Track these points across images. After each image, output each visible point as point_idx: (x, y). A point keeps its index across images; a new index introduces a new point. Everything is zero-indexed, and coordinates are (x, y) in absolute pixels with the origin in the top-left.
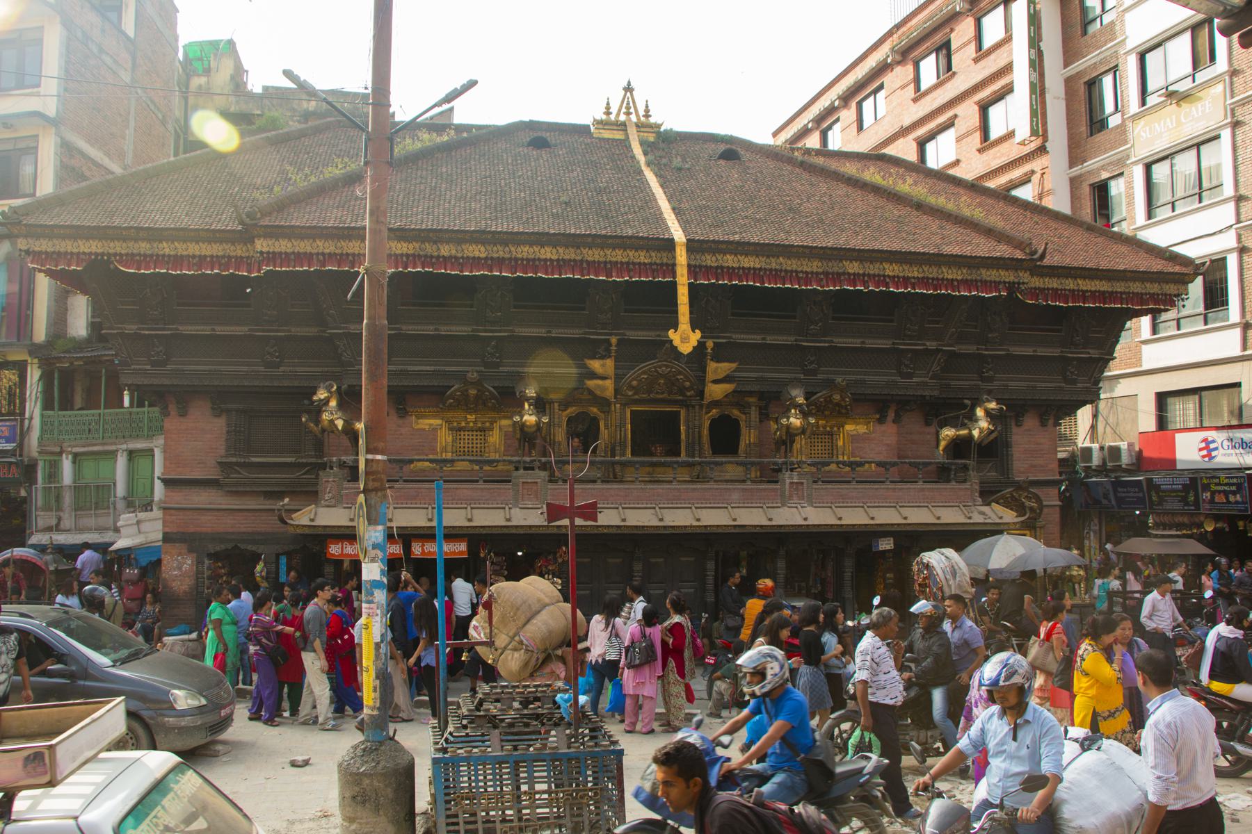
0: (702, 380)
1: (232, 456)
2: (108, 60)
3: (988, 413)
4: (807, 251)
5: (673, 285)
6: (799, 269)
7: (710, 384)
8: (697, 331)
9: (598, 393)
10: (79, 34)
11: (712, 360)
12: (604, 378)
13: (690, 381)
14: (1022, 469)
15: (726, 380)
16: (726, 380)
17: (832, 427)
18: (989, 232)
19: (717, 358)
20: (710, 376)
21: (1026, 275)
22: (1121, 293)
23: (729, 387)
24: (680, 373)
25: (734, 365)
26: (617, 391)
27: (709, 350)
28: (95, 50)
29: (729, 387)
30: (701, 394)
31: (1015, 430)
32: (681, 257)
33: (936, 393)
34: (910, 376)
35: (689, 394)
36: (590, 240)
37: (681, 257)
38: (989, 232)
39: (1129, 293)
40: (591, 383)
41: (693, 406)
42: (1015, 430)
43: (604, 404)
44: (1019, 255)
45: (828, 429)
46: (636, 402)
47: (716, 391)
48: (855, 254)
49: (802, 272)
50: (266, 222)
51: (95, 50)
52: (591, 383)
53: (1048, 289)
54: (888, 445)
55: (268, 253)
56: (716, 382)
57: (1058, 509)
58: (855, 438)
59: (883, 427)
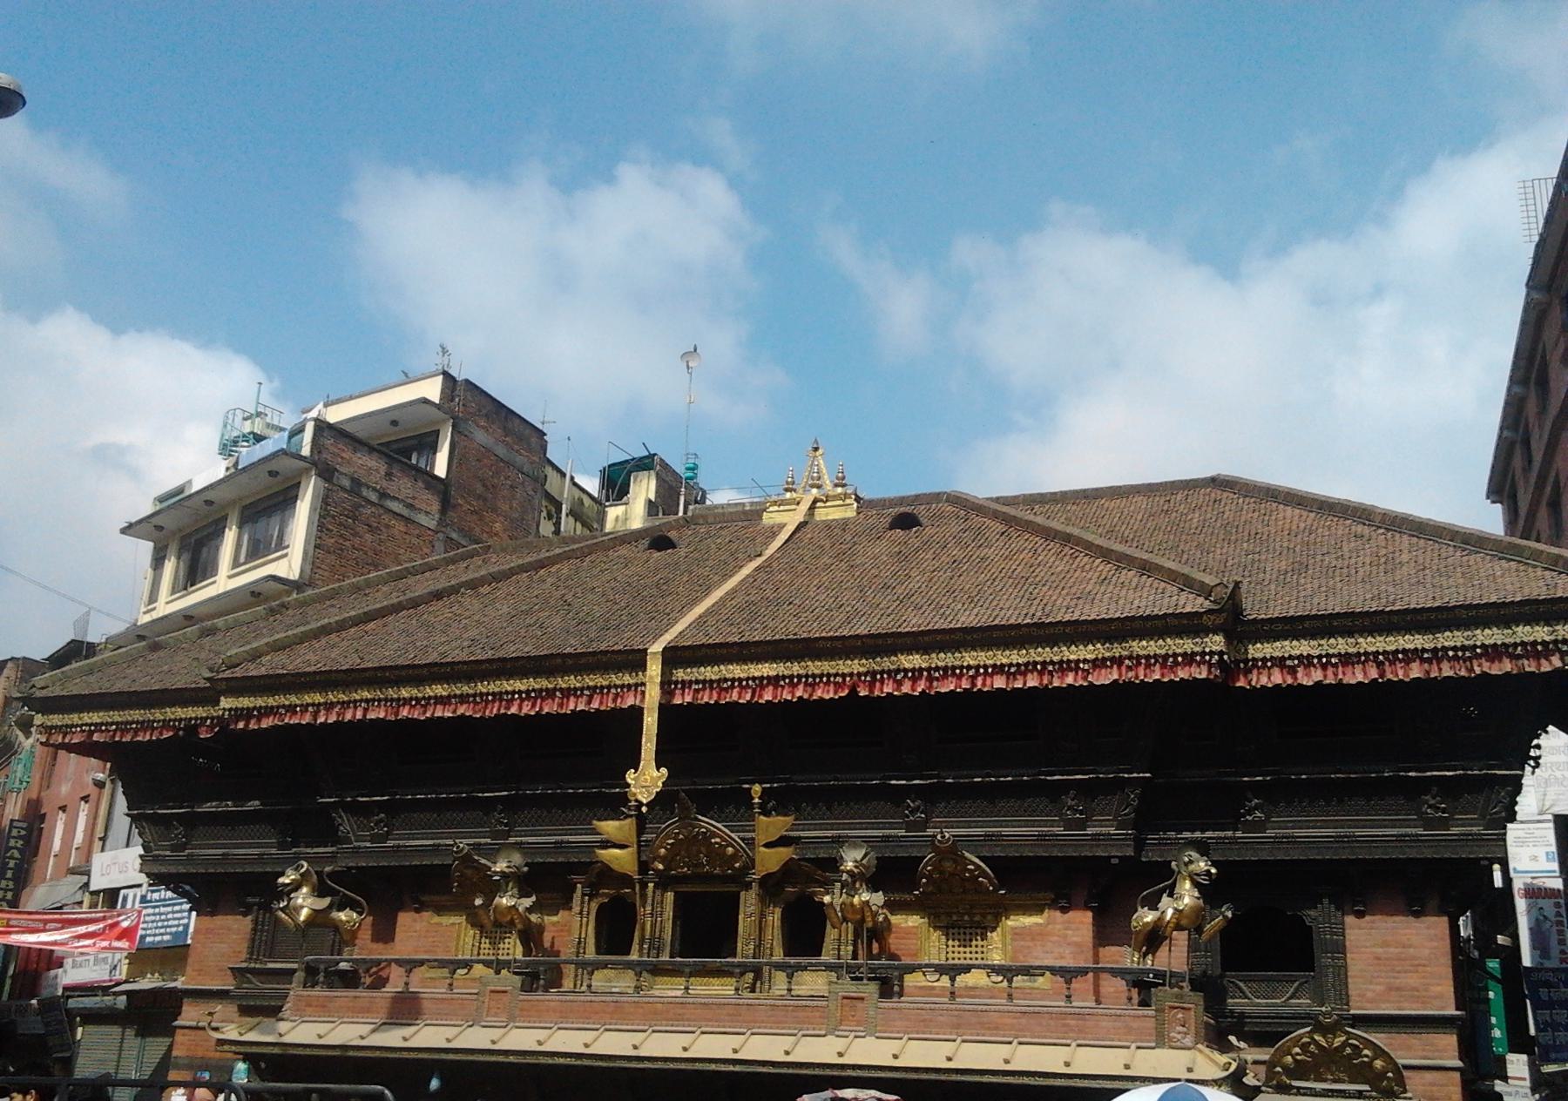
0: (750, 843)
1: (249, 960)
2: (395, 506)
3: (1196, 884)
4: (838, 644)
5: (637, 713)
6: (834, 671)
7: (762, 849)
8: (664, 770)
9: (615, 866)
10: (346, 483)
11: (760, 813)
13: (733, 846)
14: (1369, 994)
15: (783, 841)
16: (783, 841)
17: (984, 916)
18: (1172, 577)
19: (766, 813)
20: (762, 838)
22: (1455, 649)
23: (785, 853)
24: (714, 835)
25: (790, 819)
26: (644, 867)
27: (757, 800)
28: (373, 497)
29: (785, 853)
30: (750, 864)
31: (1350, 920)
32: (654, 669)
33: (1130, 852)
34: (1082, 825)
35: (737, 865)
36: (559, 661)
37: (654, 669)
38: (1172, 577)
39: (1475, 646)
41: (751, 883)
43: (625, 880)
44: (1192, 603)
45: (977, 918)
47: (770, 860)
48: (909, 641)
49: (836, 675)
50: (227, 674)
53: (1291, 657)
54: (1077, 944)
55: (230, 710)
57: (1457, 1075)
58: (1018, 933)
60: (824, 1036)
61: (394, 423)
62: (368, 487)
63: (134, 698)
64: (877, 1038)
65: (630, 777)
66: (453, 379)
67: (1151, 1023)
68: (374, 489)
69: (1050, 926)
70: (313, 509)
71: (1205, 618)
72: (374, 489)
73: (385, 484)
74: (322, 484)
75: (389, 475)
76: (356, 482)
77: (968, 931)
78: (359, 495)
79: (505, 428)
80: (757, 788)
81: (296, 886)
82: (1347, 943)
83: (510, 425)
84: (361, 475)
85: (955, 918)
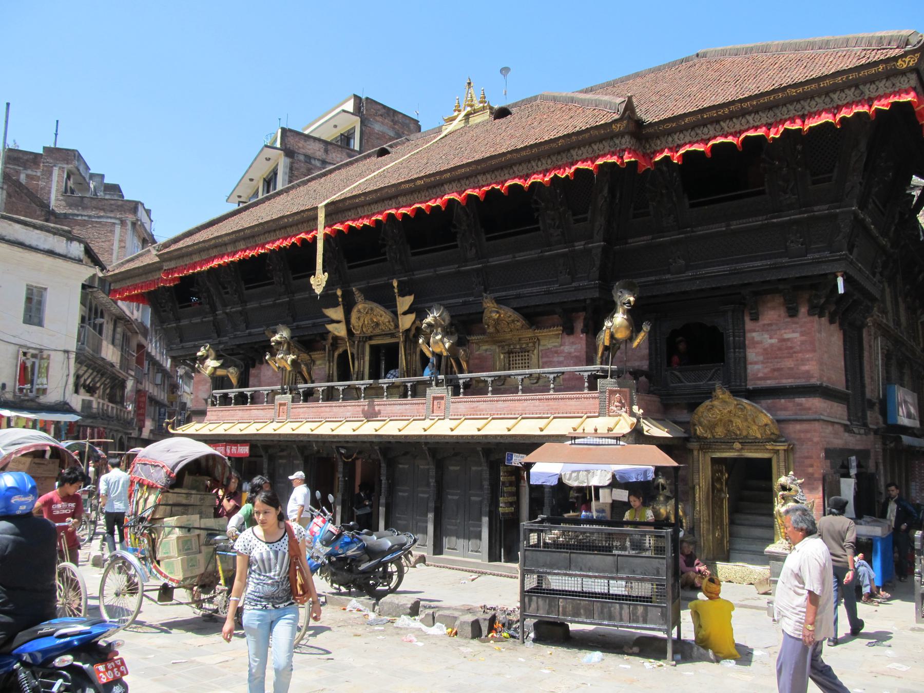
0: (395, 313)
10: (302, 158)
12: (338, 322)
17: (527, 344)
19: (403, 294)
21: (623, 141)
26: (350, 332)
30: (397, 326)
40: (330, 327)
42: (749, 324)
45: (524, 346)
46: (370, 338)
47: (406, 322)
51: (318, 164)
52: (330, 327)
56: (405, 313)
59: (571, 339)
60: (424, 420)
61: (335, 126)
62: (315, 159)
63: (141, 271)
64: (450, 419)
65: (312, 280)
66: (360, 99)
67: (597, 401)
68: (318, 160)
69: (562, 347)
70: (285, 173)
71: (614, 127)
72: (318, 160)
73: (324, 157)
74: (288, 160)
75: (326, 151)
76: (306, 156)
77: (520, 354)
78: (310, 163)
79: (393, 121)
80: (395, 284)
81: (203, 359)
82: (747, 342)
83: (396, 118)
84: (309, 152)
85: (512, 347)
